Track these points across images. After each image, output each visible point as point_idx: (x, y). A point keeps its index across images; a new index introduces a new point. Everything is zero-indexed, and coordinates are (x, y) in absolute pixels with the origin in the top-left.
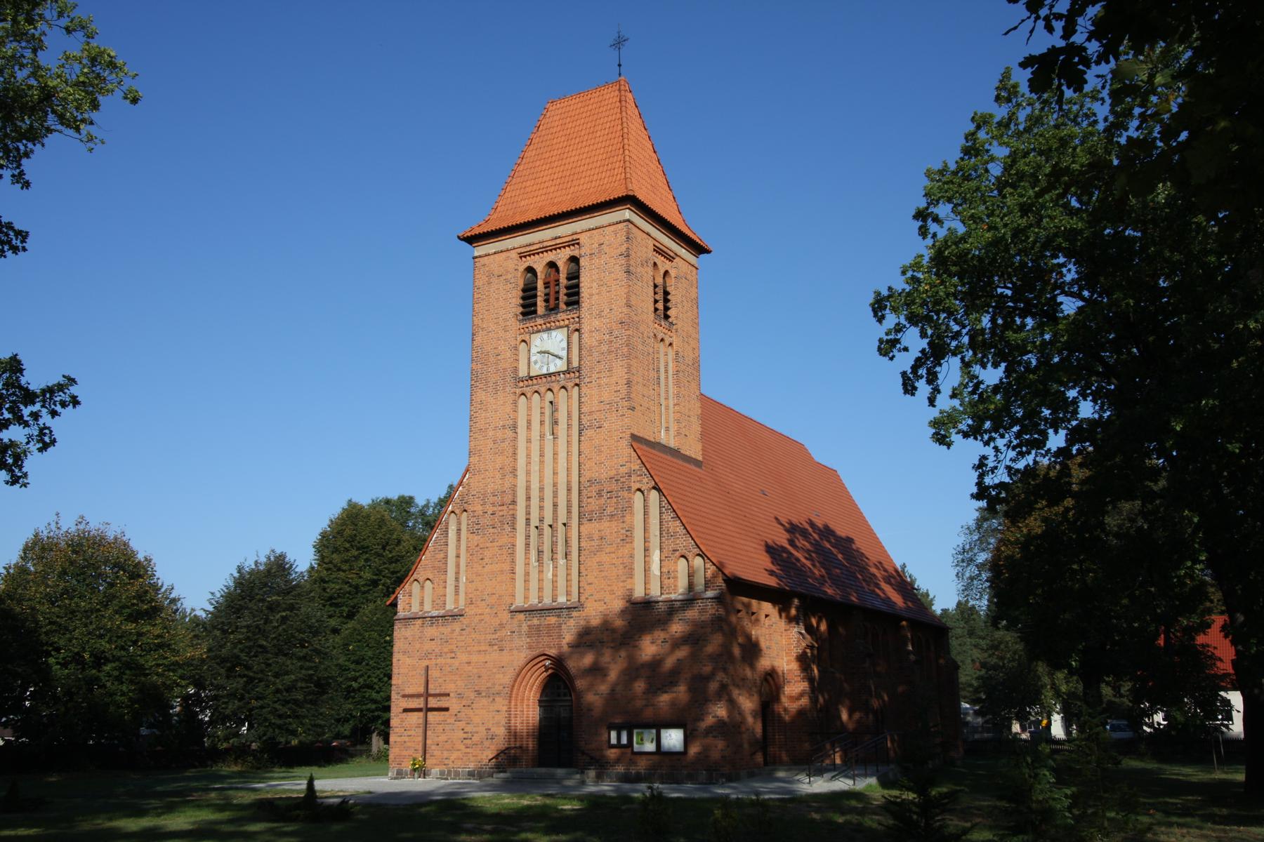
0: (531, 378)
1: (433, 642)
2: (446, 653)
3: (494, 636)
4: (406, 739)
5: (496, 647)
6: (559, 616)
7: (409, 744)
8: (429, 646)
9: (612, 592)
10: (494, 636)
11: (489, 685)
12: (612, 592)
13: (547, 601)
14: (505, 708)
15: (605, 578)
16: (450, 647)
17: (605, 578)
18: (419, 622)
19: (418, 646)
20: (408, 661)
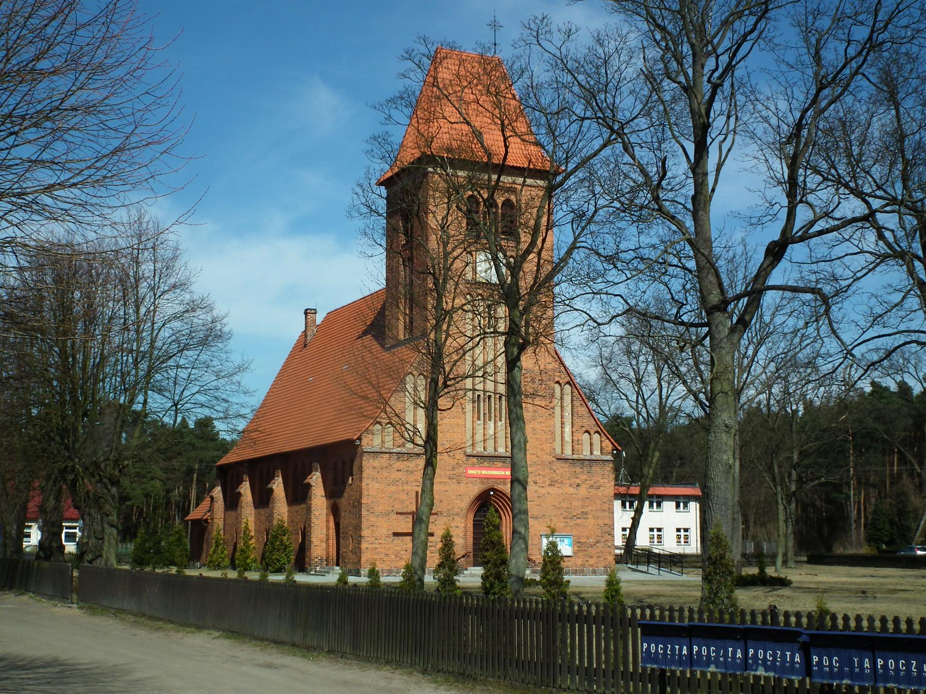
0: (476, 283)
1: (400, 473)
2: (412, 482)
3: (452, 472)
4: (377, 546)
5: (454, 481)
6: (504, 462)
7: (380, 550)
8: (395, 475)
9: (542, 450)
10: (452, 472)
11: (449, 508)
12: (542, 450)
13: (490, 451)
14: (463, 525)
15: (537, 439)
16: (415, 478)
17: (537, 439)
18: (387, 455)
19: (386, 475)
20: (377, 486)
